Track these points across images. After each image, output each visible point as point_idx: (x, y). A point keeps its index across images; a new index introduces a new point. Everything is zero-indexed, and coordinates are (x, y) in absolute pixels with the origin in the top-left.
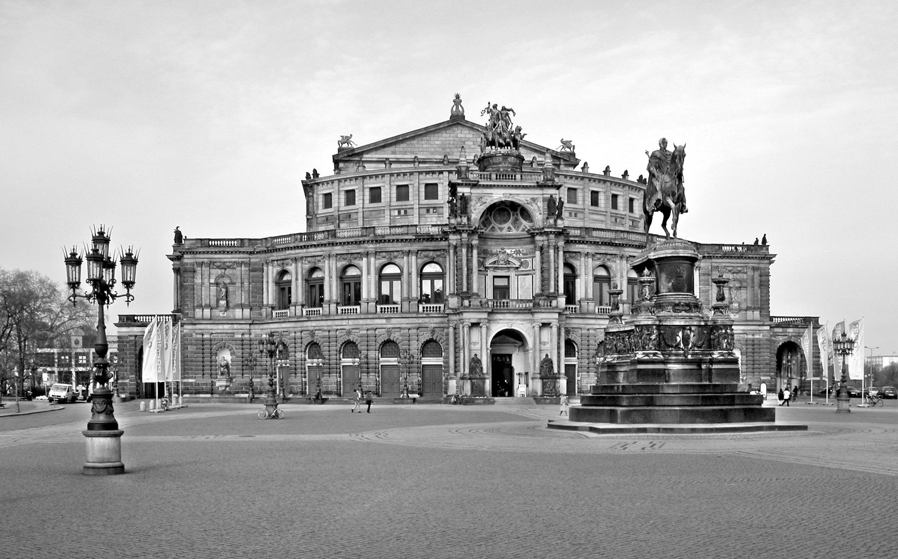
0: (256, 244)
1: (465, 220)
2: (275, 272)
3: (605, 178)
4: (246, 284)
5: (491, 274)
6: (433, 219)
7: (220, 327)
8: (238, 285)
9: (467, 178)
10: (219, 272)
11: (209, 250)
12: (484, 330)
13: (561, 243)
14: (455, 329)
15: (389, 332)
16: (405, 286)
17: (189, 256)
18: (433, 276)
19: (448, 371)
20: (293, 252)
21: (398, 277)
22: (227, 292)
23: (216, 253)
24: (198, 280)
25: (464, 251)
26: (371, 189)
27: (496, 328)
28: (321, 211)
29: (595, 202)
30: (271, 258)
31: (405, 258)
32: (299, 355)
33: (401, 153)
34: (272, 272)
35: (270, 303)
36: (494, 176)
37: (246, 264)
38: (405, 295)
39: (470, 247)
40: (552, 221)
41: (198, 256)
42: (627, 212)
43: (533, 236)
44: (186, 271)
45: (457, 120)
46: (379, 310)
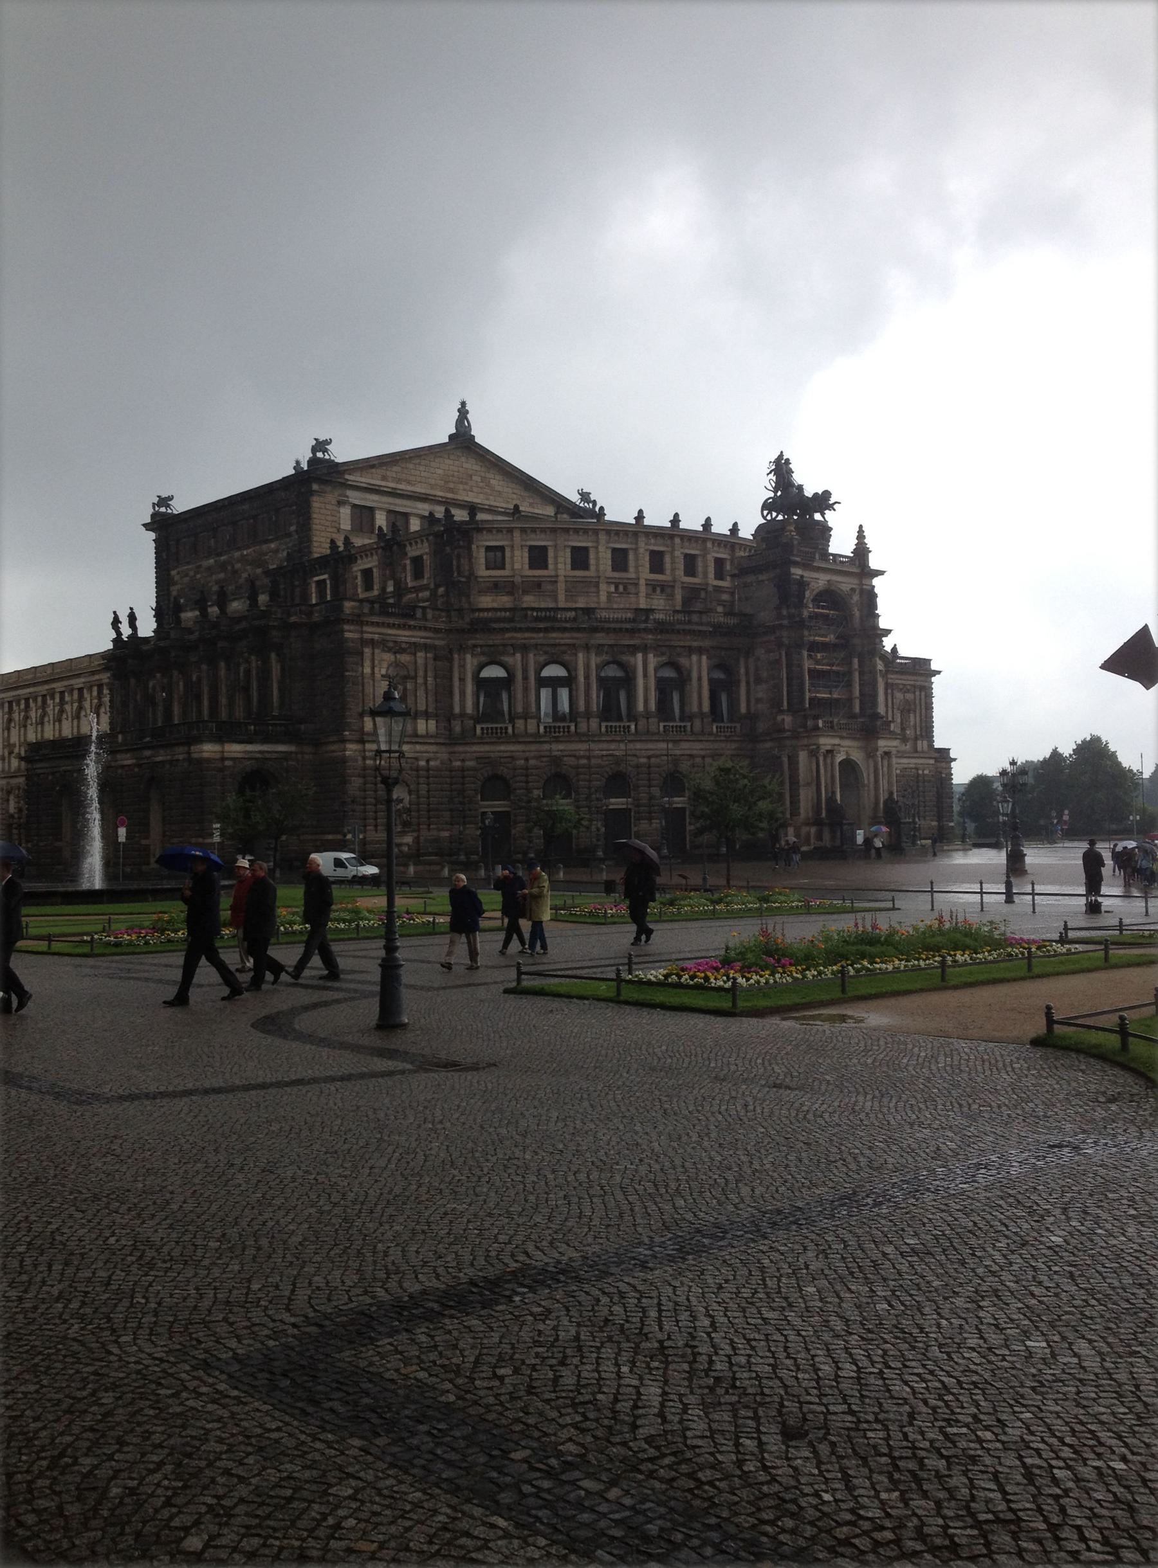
2: (475, 662)
6: (659, 602)
8: (420, 680)
17: (352, 628)
20: (519, 635)
23: (393, 626)
24: (367, 670)
26: (574, 548)
27: (840, 758)
28: (482, 572)
30: (470, 642)
31: (694, 658)
34: (471, 662)
37: (426, 647)
38: (695, 709)
41: (365, 628)
45: (462, 440)
46: (661, 728)
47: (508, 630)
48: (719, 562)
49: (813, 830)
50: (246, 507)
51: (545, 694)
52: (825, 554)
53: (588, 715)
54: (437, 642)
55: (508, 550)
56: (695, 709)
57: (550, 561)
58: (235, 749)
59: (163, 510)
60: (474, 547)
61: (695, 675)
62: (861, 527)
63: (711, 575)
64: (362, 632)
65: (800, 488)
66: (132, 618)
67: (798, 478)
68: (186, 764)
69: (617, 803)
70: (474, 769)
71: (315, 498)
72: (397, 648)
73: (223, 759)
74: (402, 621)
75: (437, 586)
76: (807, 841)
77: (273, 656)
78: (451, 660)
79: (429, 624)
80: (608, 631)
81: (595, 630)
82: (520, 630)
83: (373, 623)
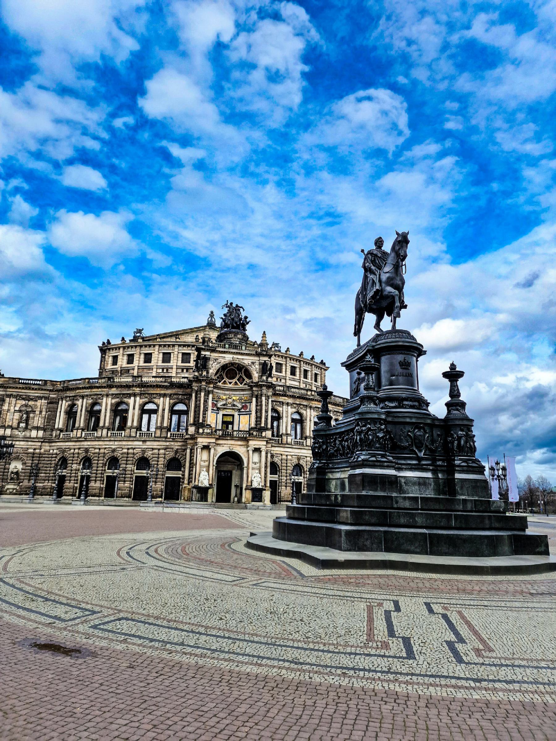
1: (205, 373)
2: (67, 404)
3: (300, 359)
4: (44, 413)
5: (221, 413)
8: (37, 413)
9: (208, 346)
10: (24, 402)
11: (18, 386)
12: (212, 451)
13: (270, 394)
14: (191, 450)
15: (144, 451)
16: (159, 419)
18: (180, 413)
19: (183, 482)
20: (81, 391)
21: (155, 412)
23: (23, 388)
24: (5, 407)
25: (203, 394)
27: (221, 450)
28: (109, 366)
29: (293, 373)
31: (162, 399)
32: (75, 466)
34: (64, 405)
35: (60, 426)
36: (227, 346)
38: (159, 425)
39: (207, 393)
40: (264, 378)
42: (313, 382)
43: (251, 387)
46: (138, 435)
53: (103, 427)
60: (107, 357)
70: (56, 454)
72: (28, 398)
80: (117, 387)
81: (110, 387)
83: (10, 388)
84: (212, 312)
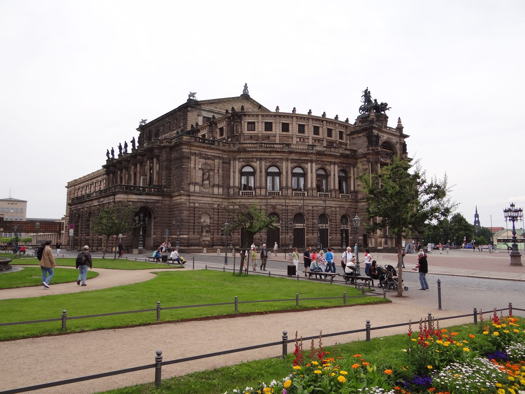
0: (226, 146)
2: (240, 165)
7: (205, 199)
8: (216, 171)
10: (204, 161)
15: (325, 208)
20: (259, 154)
22: (209, 175)
26: (283, 124)
28: (246, 132)
30: (238, 157)
31: (332, 166)
33: (219, 108)
34: (238, 165)
38: (332, 188)
41: (192, 148)
44: (184, 157)
45: (245, 96)
46: (318, 195)
47: (254, 151)
48: (341, 133)
49: (383, 240)
50: (167, 119)
51: (269, 179)
52: (386, 127)
54: (224, 156)
55: (256, 123)
56: (332, 188)
57: (273, 128)
58: (134, 197)
59: (143, 124)
60: (243, 122)
61: (332, 173)
62: (399, 118)
63: (338, 137)
64: (191, 149)
65: (375, 100)
66: (113, 151)
67: (372, 99)
68: (113, 203)
69: (299, 226)
71: (188, 113)
72: (207, 158)
73: (128, 201)
74: (209, 145)
75: (228, 138)
76: (380, 245)
77: (155, 160)
78: (229, 164)
79: (221, 148)
81: (291, 152)
82: (259, 152)
84: (246, 84)
